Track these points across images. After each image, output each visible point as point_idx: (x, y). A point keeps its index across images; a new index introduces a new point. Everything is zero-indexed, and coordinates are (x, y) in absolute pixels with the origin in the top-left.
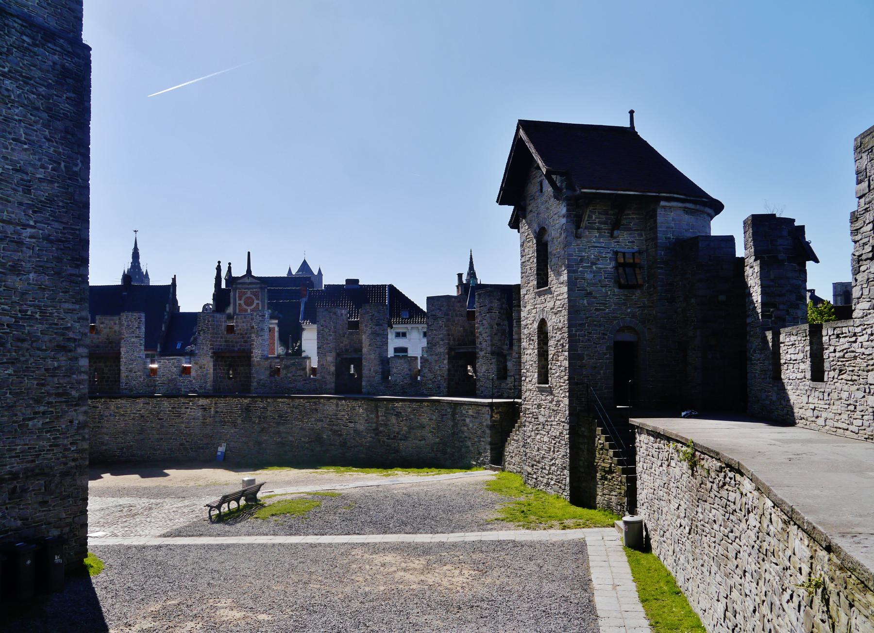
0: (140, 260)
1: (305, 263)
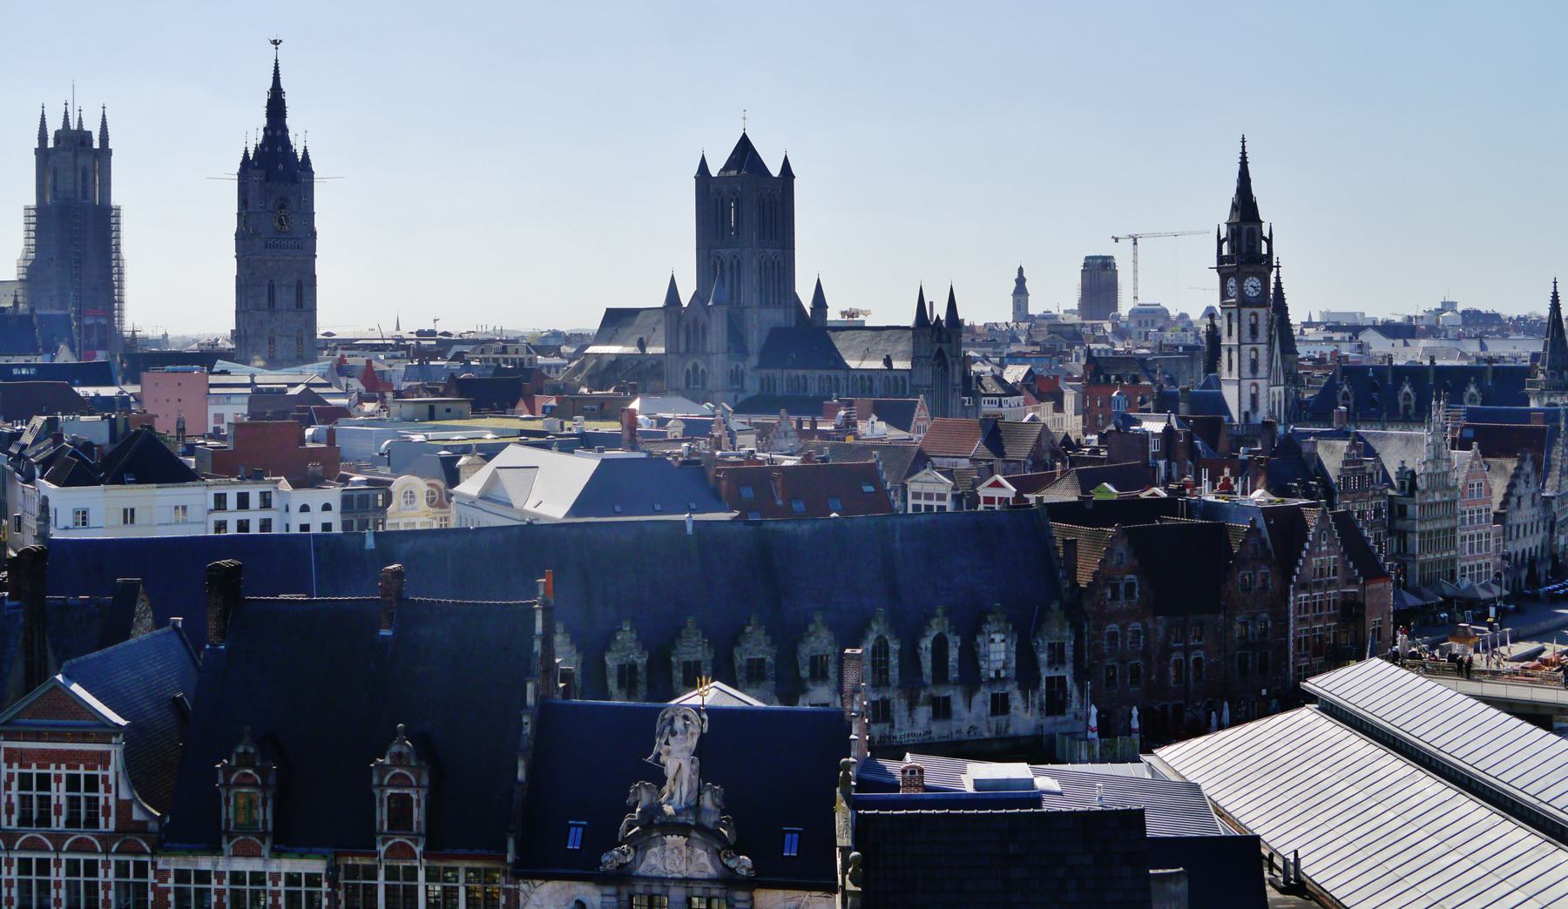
0: (288, 122)
1: (744, 146)
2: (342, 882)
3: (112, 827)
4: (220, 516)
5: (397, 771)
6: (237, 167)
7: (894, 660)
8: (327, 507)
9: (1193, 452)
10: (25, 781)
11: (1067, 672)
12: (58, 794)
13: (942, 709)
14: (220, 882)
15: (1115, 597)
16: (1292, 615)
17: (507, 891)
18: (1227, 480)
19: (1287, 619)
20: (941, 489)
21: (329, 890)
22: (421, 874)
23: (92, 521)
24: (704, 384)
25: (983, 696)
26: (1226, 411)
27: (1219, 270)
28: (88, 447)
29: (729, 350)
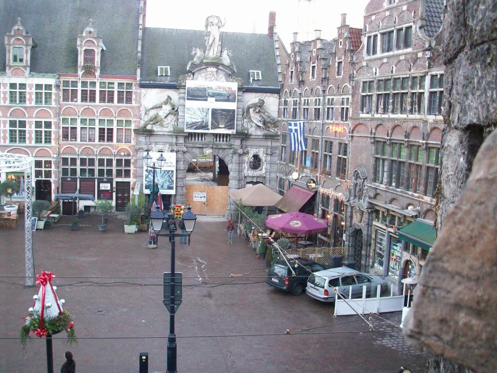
2: (62, 88)
5: (89, 39)
21: (56, 92)
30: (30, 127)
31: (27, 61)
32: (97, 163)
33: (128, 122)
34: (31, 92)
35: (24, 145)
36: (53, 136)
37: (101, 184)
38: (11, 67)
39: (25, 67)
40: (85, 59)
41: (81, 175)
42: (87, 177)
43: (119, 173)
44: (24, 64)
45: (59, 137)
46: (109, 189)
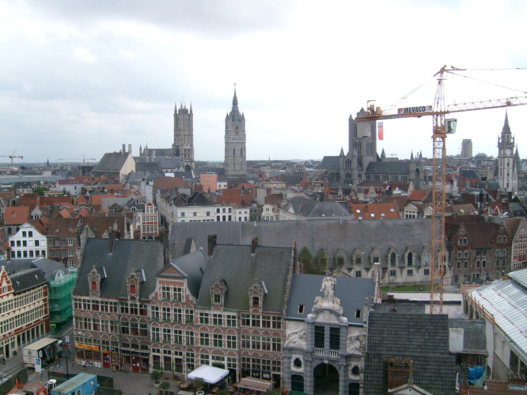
0: (239, 106)
2: (241, 318)
3: (184, 301)
4: (218, 214)
6: (225, 118)
7: (397, 259)
8: (246, 212)
9: (488, 200)
10: (164, 288)
11: (446, 264)
12: (172, 292)
13: (410, 272)
14: (211, 316)
15: (461, 243)
16: (512, 250)
17: (283, 323)
18: (497, 209)
19: (511, 251)
20: (414, 210)
22: (261, 317)
23: (186, 215)
24: (350, 177)
25: (422, 271)
26: (499, 187)
27: (498, 147)
28: (185, 196)
29: (358, 168)
30: (225, 339)
31: (222, 302)
32: (261, 362)
33: (279, 340)
34: (225, 319)
35: (221, 348)
36: (237, 345)
37: (264, 375)
38: (213, 305)
39: (221, 306)
40: (253, 302)
41: (253, 368)
42: (256, 369)
43: (274, 369)
44: (220, 304)
45: (240, 345)
46: (268, 377)
